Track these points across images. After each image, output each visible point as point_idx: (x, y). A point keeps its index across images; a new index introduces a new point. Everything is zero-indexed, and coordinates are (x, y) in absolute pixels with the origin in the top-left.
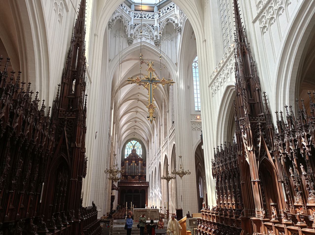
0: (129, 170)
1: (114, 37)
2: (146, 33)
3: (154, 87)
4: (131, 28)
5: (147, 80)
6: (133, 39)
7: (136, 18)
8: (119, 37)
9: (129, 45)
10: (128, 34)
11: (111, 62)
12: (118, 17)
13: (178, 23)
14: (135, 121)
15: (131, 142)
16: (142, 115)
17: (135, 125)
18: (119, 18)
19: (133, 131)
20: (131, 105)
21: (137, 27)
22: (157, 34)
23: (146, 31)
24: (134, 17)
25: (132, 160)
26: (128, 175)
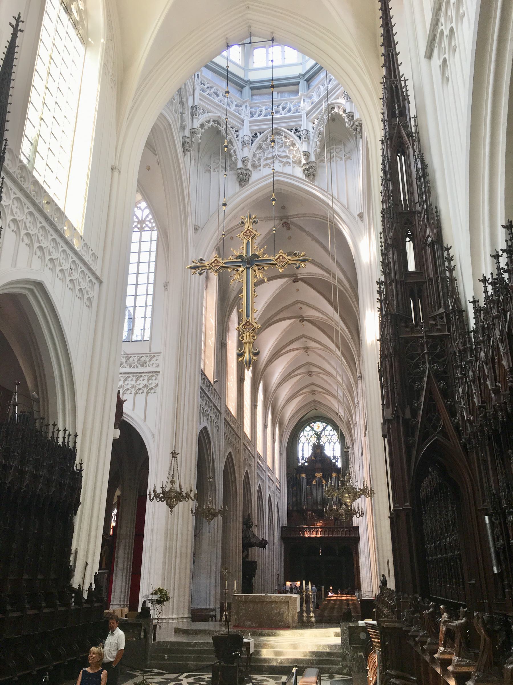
0: (309, 498)
1: (205, 172)
2: (281, 150)
3: (255, 277)
4: (244, 144)
5: (240, 260)
6: (248, 169)
7: (255, 118)
8: (216, 170)
9: (241, 186)
10: (236, 159)
11: (199, 231)
12: (208, 122)
13: (354, 111)
14: (308, 372)
15: (311, 427)
16: (320, 356)
17: (313, 384)
18: (211, 125)
19: (311, 398)
20: (288, 332)
21: (258, 139)
22: (308, 148)
23: (282, 146)
24: (252, 116)
25: (315, 471)
26: (308, 510)
